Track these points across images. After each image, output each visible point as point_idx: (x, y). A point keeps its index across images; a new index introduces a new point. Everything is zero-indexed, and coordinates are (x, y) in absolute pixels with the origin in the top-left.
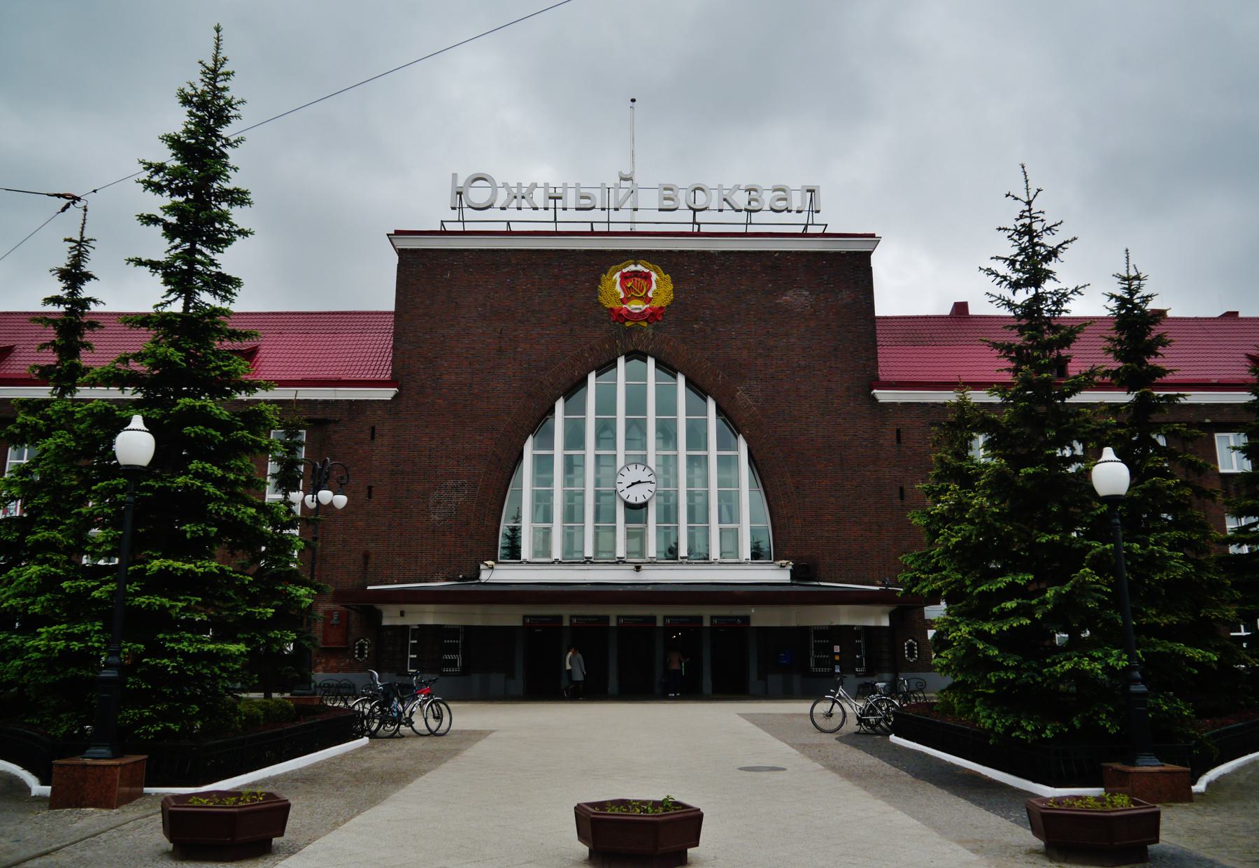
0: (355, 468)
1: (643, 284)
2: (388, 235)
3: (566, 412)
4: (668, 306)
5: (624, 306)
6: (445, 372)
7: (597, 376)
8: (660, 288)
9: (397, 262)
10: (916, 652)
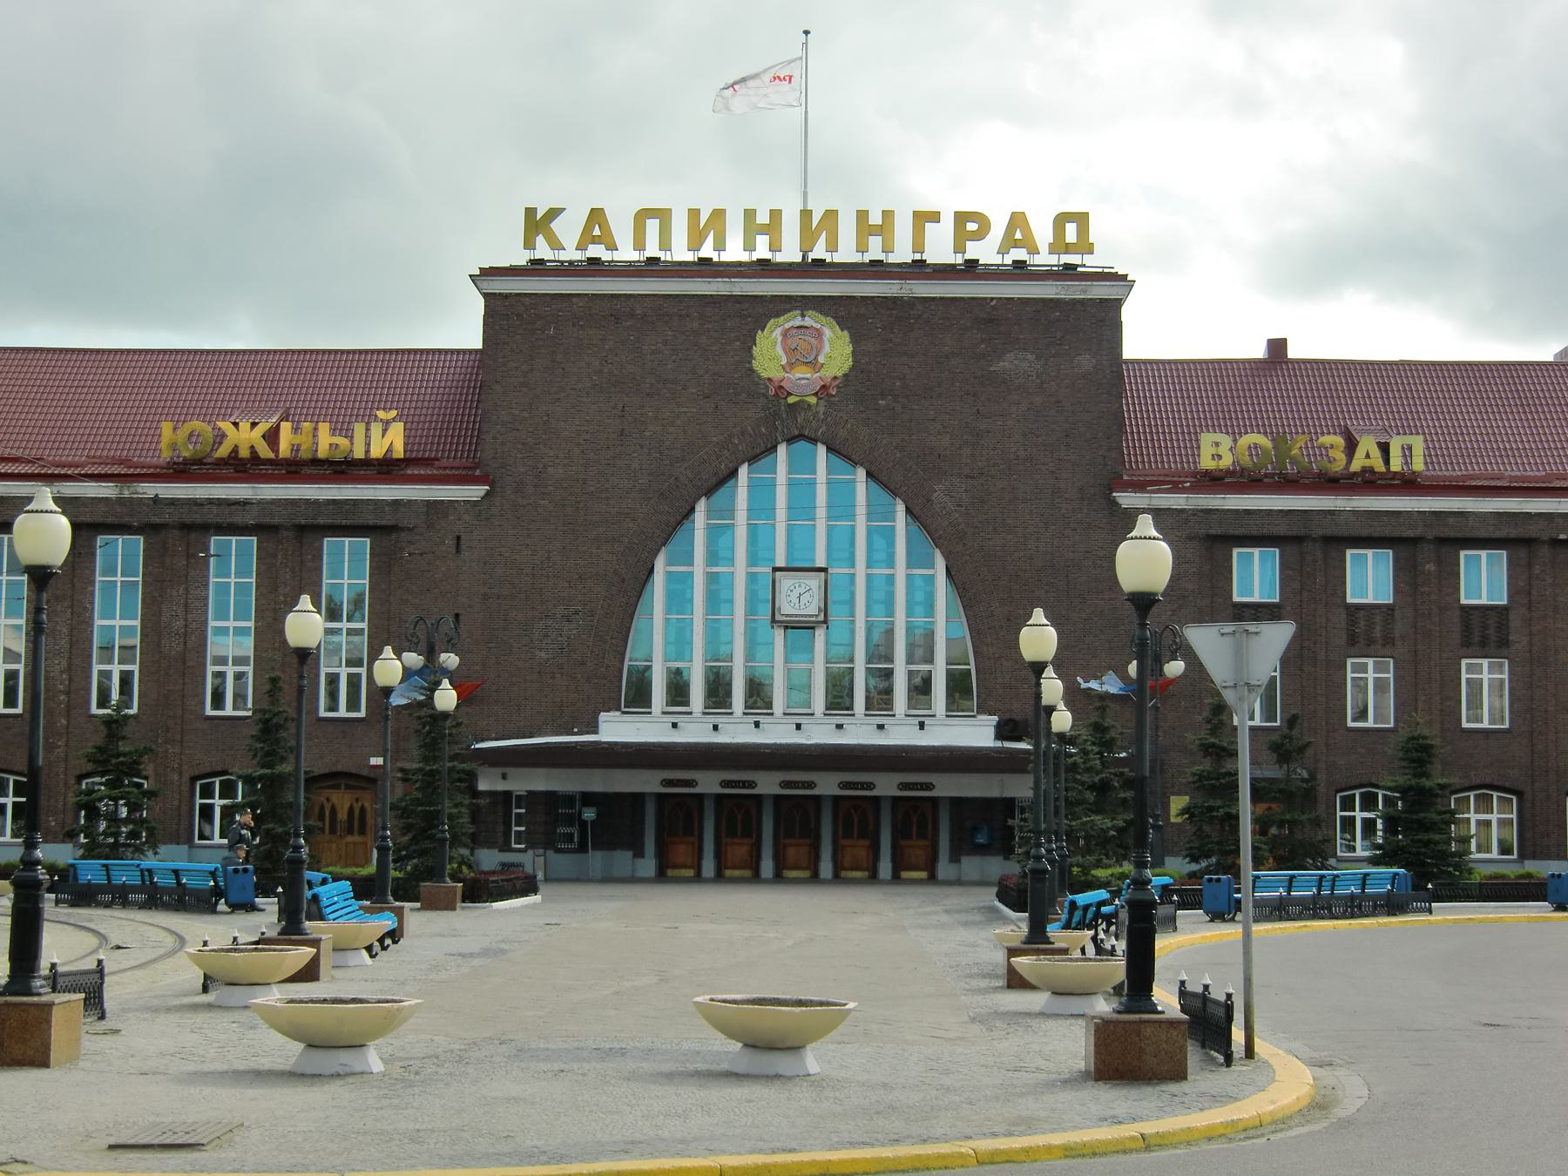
0: (436, 590)
2: (470, 276)
3: (710, 514)
4: (845, 375)
6: (550, 464)
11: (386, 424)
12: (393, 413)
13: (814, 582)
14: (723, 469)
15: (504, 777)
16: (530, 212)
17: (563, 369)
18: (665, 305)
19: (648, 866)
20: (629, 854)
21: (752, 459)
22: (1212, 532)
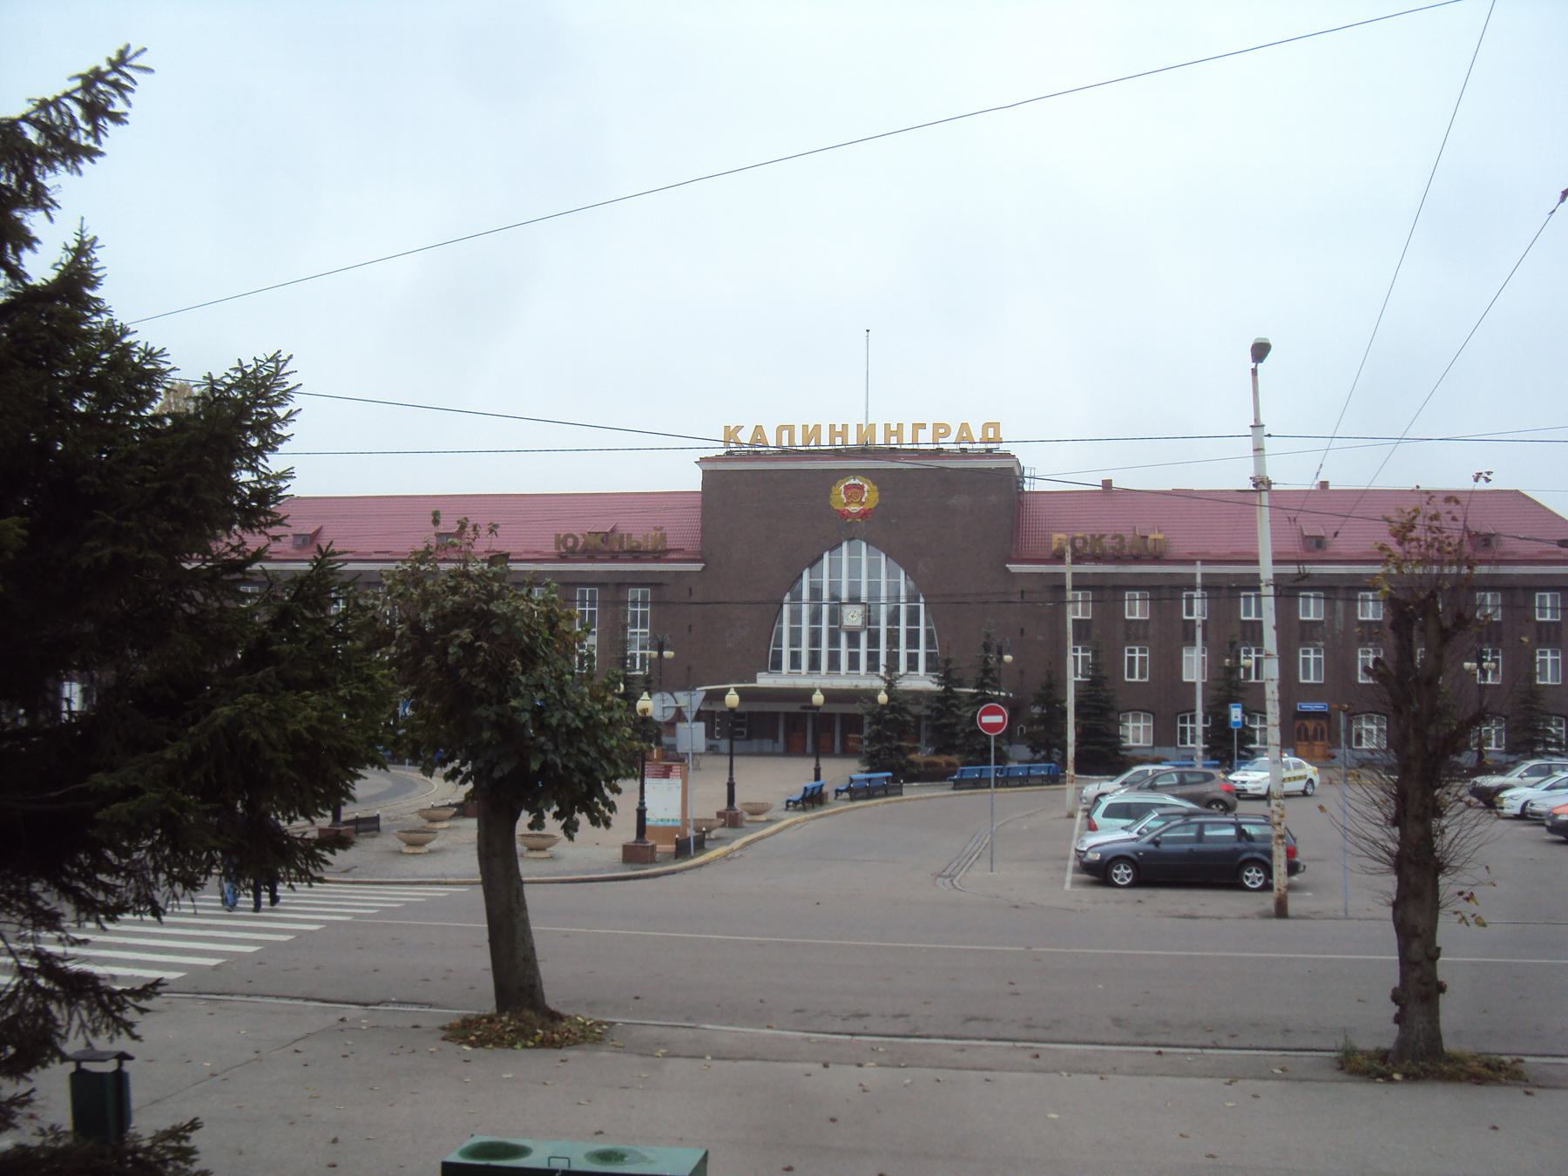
8: (870, 495)
19: (780, 746)
20: (771, 741)
21: (831, 550)
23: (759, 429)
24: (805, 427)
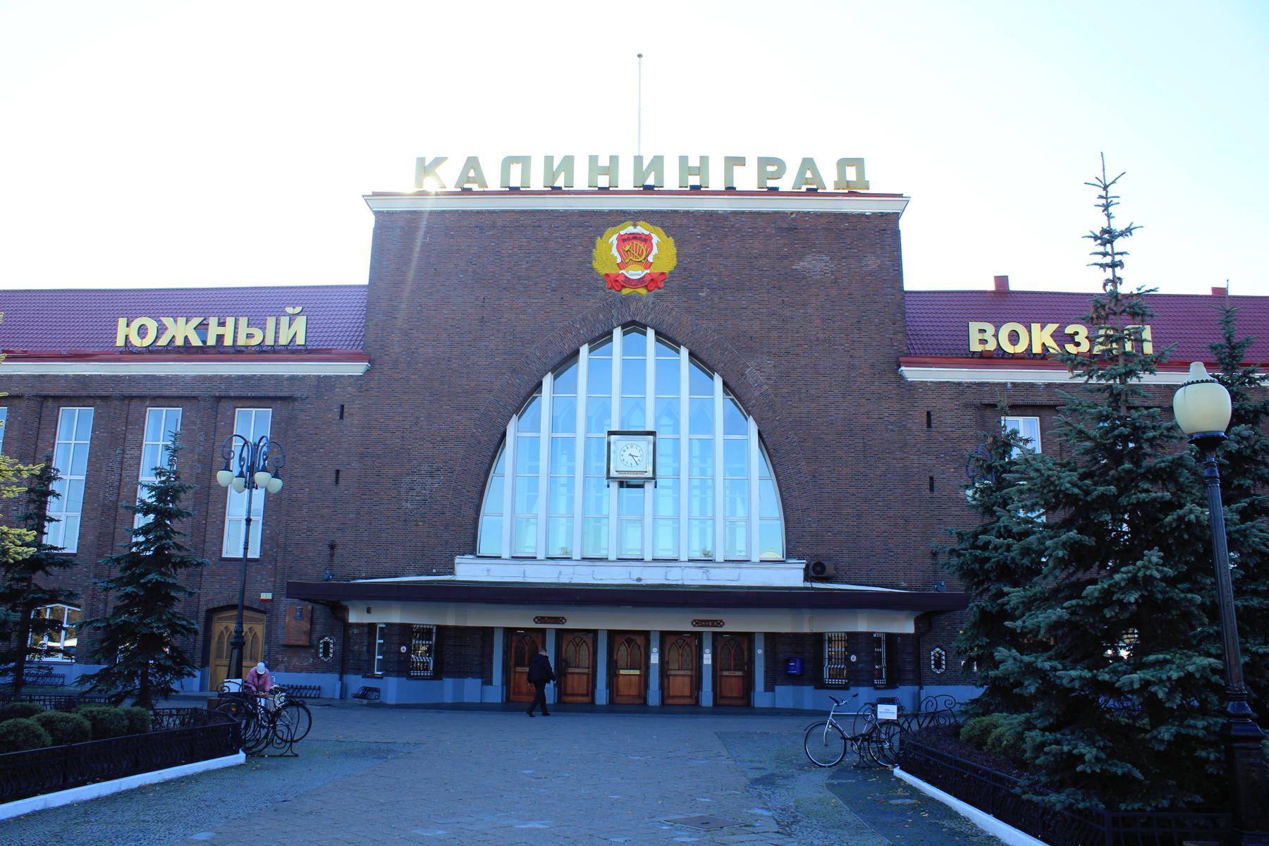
0: (322, 450)
1: (642, 247)
5: (621, 272)
6: (421, 345)
7: (591, 351)
9: (373, 226)
10: (944, 662)
11: (292, 318)
12: (298, 309)
13: (645, 444)
14: (567, 350)
15: (369, 611)
16: (421, 161)
17: (435, 269)
18: (522, 219)
20: (479, 681)
22: (986, 402)
23: (472, 162)
24: (549, 160)
